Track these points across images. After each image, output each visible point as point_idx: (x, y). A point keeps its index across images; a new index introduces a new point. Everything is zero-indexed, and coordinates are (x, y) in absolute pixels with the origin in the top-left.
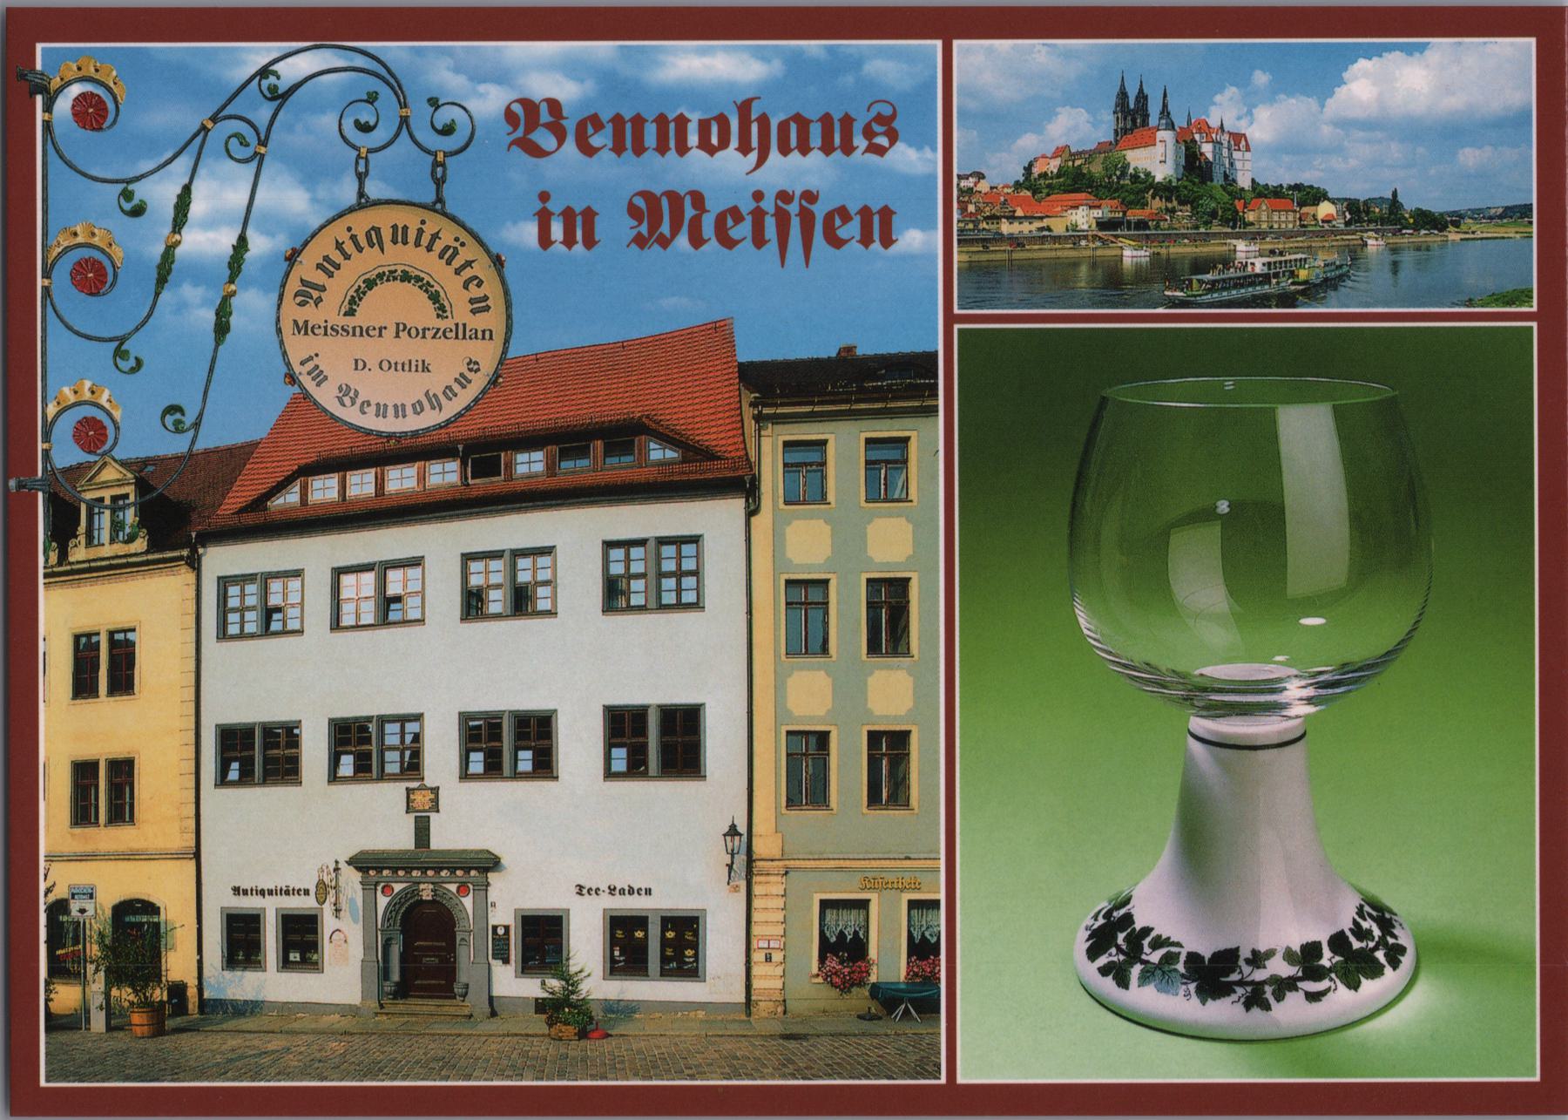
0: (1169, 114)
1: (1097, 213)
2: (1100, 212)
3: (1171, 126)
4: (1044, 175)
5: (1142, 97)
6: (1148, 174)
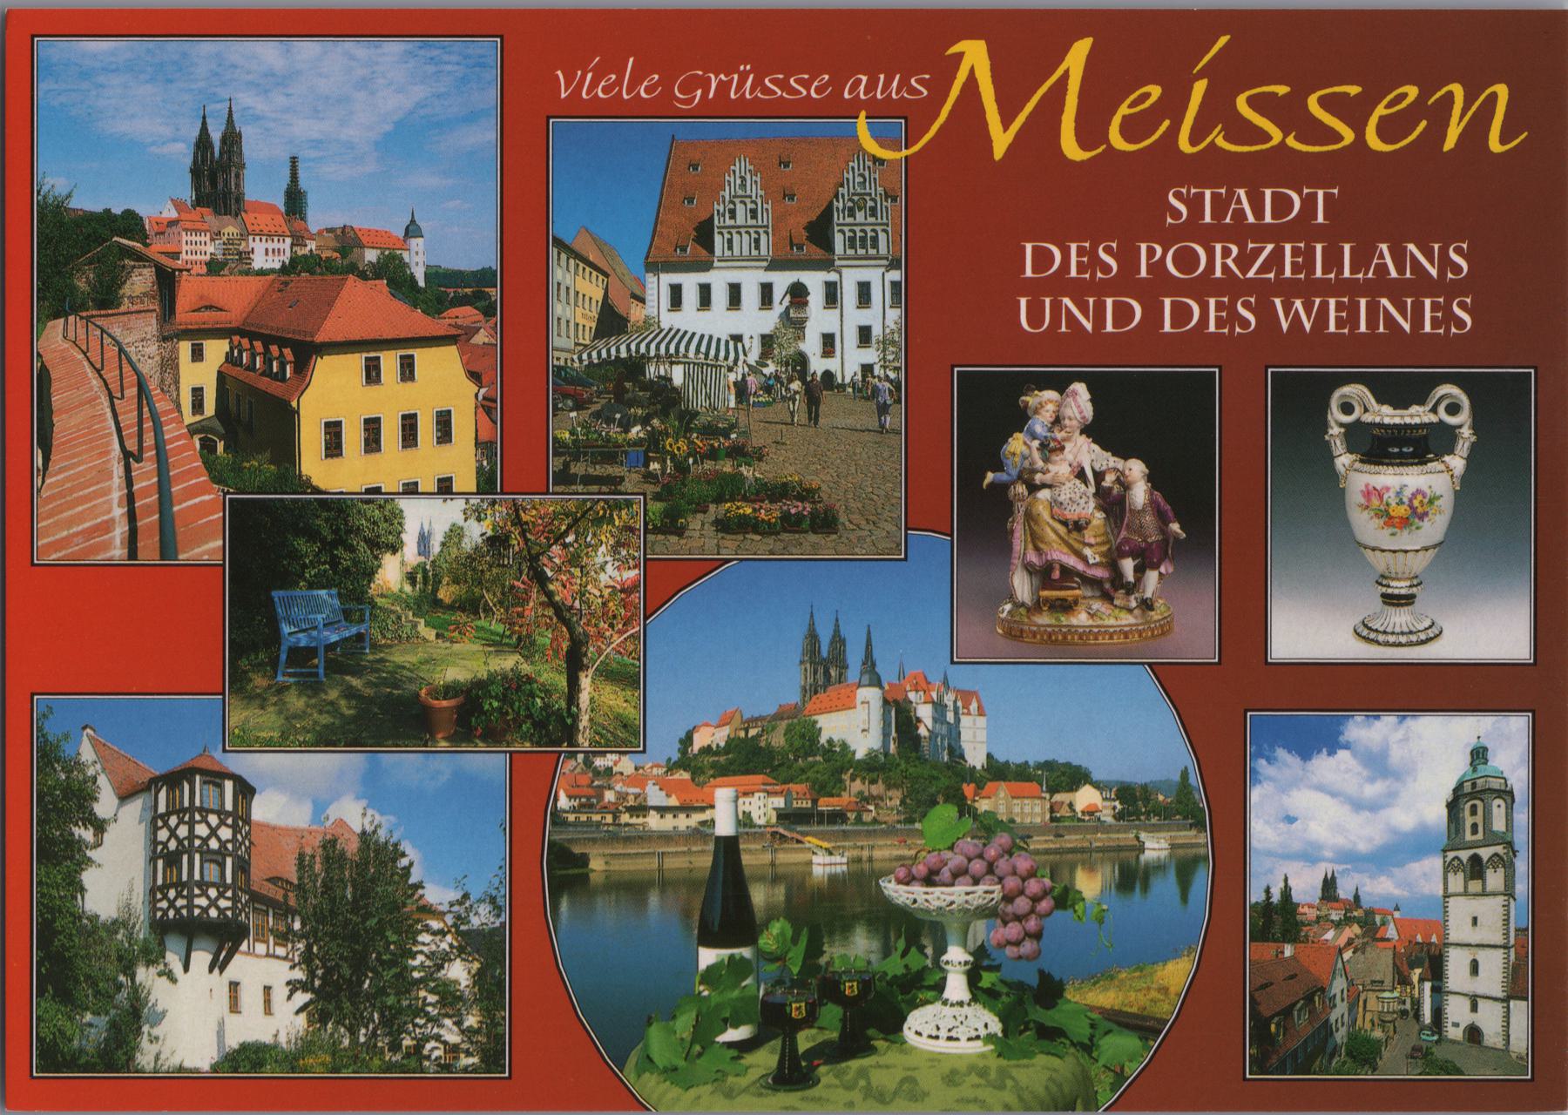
0: (874, 665)
1: (779, 802)
3: (876, 682)
4: (707, 750)
5: (838, 641)
6: (844, 745)
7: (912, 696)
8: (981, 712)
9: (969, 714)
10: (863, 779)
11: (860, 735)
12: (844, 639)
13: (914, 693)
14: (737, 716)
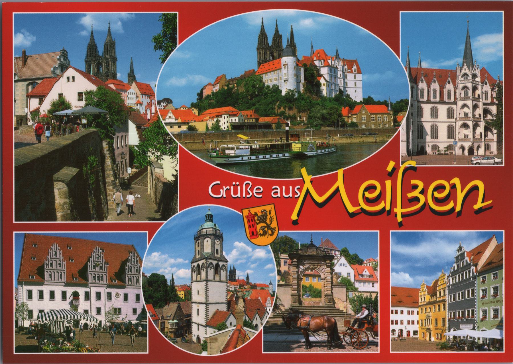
1: (235, 120)
2: (237, 118)
7: (317, 63)
8: (359, 71)
9: (352, 72)
10: (285, 108)
11: (284, 83)
12: (281, 36)
13: (318, 61)
14: (223, 79)
